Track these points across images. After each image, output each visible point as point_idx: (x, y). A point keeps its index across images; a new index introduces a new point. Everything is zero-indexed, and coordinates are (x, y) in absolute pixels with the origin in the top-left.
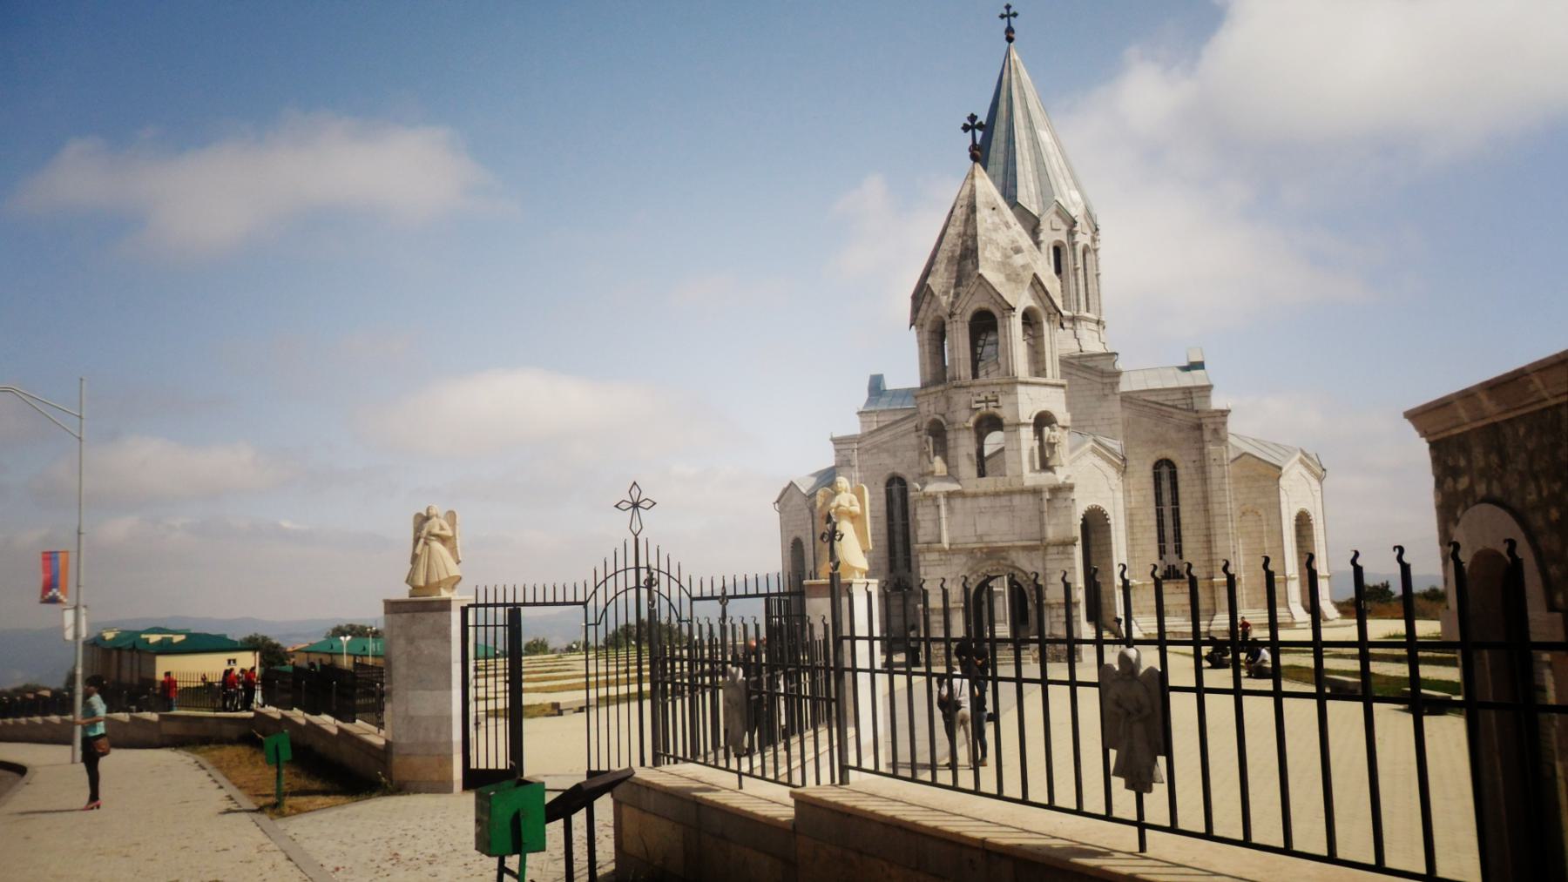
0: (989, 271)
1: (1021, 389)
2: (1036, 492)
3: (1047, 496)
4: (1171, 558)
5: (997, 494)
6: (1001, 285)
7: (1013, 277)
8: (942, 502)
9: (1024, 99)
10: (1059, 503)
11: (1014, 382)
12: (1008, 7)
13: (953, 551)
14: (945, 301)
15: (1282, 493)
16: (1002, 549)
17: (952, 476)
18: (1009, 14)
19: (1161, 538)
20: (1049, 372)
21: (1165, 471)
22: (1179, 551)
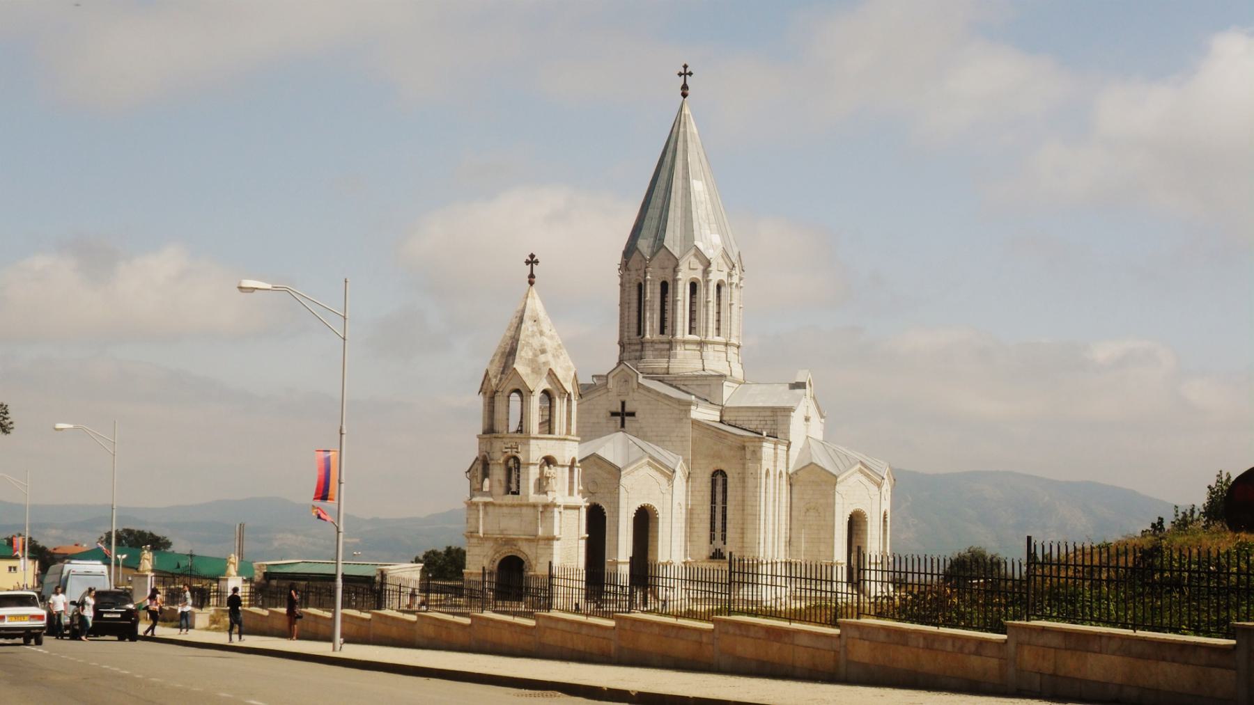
0: (520, 367)
1: (532, 442)
2: (535, 506)
3: (540, 509)
4: (718, 543)
5: (513, 506)
6: (527, 375)
7: (536, 371)
8: (481, 508)
9: (685, 151)
10: (547, 514)
11: (529, 438)
12: (685, 67)
13: (485, 539)
14: (494, 381)
15: (837, 496)
16: (514, 540)
17: (490, 494)
18: (685, 73)
19: (712, 529)
20: (557, 430)
21: (720, 479)
22: (724, 538)
